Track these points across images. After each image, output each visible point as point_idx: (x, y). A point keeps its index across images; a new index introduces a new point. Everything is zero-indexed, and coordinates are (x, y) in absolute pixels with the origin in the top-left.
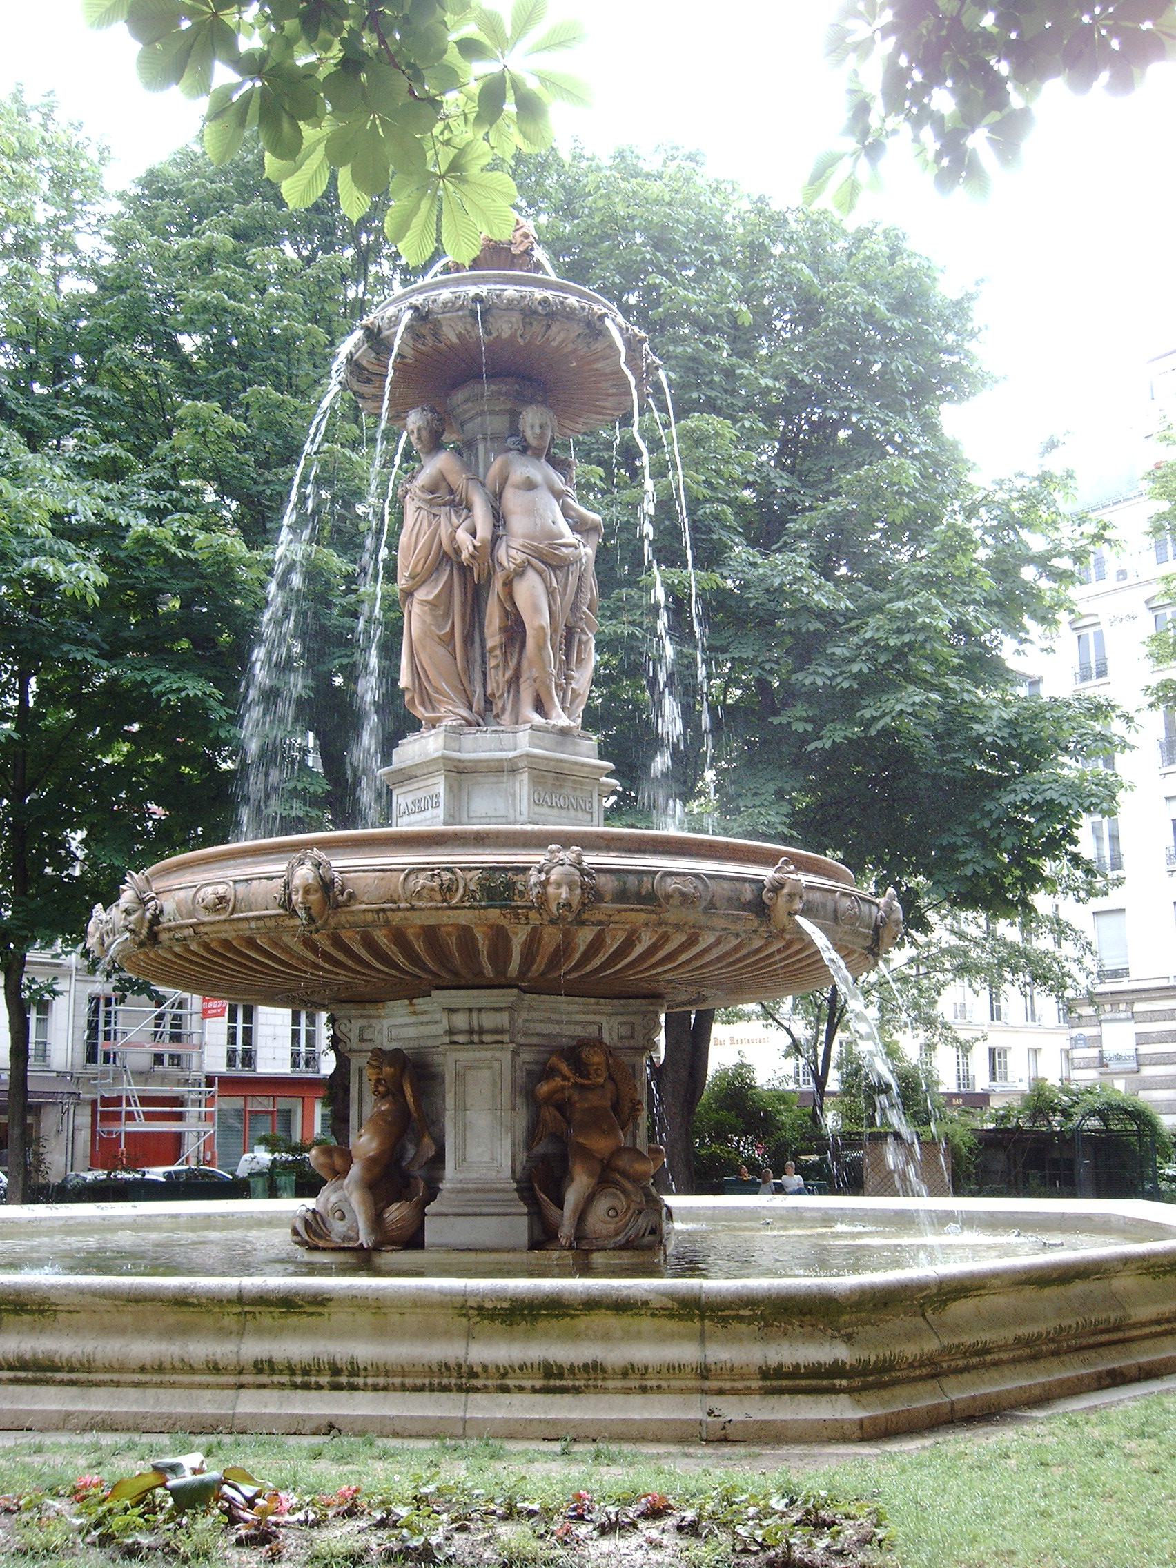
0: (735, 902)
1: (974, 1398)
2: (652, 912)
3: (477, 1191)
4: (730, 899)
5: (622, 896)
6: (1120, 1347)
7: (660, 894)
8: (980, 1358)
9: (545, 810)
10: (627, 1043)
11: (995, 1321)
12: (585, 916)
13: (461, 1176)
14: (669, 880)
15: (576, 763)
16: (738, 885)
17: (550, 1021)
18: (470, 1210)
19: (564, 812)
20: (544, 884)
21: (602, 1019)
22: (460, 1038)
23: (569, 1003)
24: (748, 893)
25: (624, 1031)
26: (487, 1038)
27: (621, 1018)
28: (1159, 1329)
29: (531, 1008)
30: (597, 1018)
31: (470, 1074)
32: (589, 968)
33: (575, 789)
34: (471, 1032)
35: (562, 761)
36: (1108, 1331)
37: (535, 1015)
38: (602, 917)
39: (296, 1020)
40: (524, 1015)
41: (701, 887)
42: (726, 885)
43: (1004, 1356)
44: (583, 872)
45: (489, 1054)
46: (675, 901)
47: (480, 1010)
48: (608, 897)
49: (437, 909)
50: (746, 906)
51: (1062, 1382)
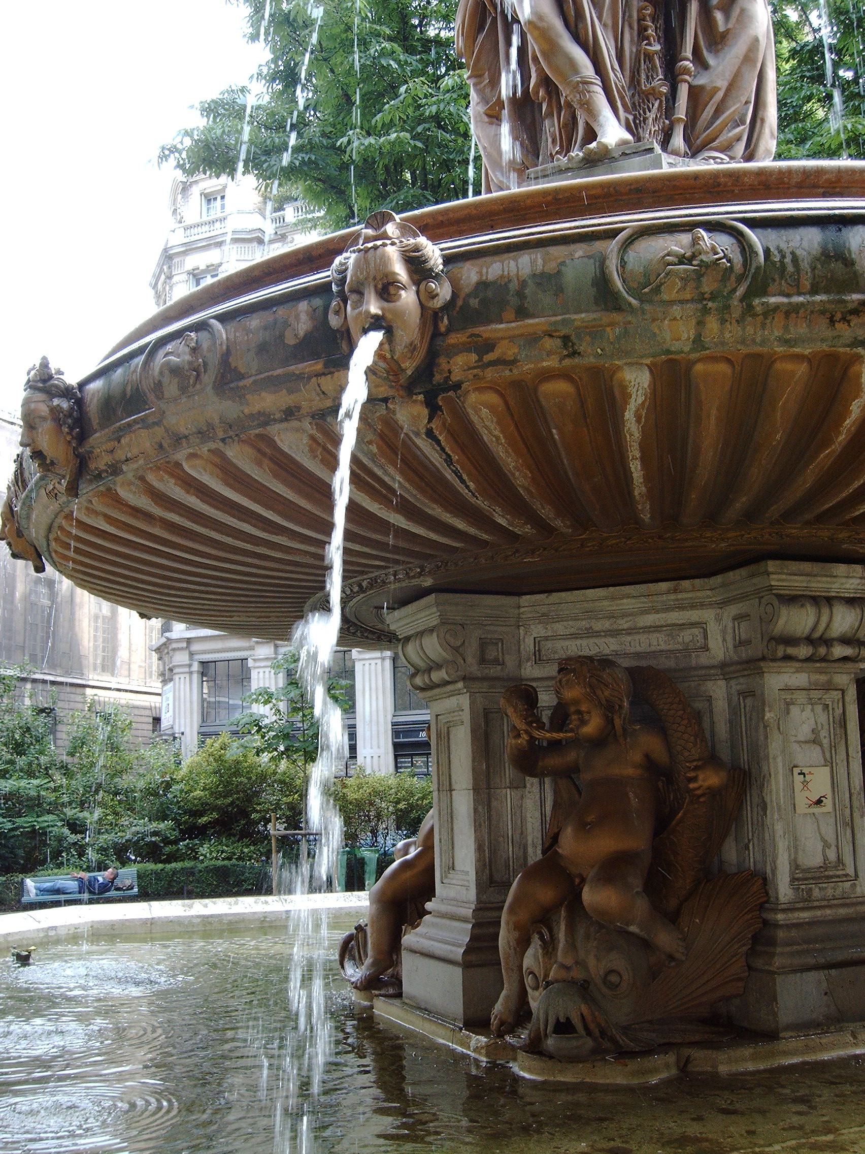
4: (262, 348)
10: (745, 653)
16: (281, 311)
17: (590, 633)
21: (708, 615)
23: (613, 598)
24: (301, 319)
25: (744, 630)
27: (734, 610)
29: (545, 618)
30: (694, 615)
31: (453, 731)
37: (560, 628)
40: (538, 630)
45: (451, 703)
46: (171, 389)
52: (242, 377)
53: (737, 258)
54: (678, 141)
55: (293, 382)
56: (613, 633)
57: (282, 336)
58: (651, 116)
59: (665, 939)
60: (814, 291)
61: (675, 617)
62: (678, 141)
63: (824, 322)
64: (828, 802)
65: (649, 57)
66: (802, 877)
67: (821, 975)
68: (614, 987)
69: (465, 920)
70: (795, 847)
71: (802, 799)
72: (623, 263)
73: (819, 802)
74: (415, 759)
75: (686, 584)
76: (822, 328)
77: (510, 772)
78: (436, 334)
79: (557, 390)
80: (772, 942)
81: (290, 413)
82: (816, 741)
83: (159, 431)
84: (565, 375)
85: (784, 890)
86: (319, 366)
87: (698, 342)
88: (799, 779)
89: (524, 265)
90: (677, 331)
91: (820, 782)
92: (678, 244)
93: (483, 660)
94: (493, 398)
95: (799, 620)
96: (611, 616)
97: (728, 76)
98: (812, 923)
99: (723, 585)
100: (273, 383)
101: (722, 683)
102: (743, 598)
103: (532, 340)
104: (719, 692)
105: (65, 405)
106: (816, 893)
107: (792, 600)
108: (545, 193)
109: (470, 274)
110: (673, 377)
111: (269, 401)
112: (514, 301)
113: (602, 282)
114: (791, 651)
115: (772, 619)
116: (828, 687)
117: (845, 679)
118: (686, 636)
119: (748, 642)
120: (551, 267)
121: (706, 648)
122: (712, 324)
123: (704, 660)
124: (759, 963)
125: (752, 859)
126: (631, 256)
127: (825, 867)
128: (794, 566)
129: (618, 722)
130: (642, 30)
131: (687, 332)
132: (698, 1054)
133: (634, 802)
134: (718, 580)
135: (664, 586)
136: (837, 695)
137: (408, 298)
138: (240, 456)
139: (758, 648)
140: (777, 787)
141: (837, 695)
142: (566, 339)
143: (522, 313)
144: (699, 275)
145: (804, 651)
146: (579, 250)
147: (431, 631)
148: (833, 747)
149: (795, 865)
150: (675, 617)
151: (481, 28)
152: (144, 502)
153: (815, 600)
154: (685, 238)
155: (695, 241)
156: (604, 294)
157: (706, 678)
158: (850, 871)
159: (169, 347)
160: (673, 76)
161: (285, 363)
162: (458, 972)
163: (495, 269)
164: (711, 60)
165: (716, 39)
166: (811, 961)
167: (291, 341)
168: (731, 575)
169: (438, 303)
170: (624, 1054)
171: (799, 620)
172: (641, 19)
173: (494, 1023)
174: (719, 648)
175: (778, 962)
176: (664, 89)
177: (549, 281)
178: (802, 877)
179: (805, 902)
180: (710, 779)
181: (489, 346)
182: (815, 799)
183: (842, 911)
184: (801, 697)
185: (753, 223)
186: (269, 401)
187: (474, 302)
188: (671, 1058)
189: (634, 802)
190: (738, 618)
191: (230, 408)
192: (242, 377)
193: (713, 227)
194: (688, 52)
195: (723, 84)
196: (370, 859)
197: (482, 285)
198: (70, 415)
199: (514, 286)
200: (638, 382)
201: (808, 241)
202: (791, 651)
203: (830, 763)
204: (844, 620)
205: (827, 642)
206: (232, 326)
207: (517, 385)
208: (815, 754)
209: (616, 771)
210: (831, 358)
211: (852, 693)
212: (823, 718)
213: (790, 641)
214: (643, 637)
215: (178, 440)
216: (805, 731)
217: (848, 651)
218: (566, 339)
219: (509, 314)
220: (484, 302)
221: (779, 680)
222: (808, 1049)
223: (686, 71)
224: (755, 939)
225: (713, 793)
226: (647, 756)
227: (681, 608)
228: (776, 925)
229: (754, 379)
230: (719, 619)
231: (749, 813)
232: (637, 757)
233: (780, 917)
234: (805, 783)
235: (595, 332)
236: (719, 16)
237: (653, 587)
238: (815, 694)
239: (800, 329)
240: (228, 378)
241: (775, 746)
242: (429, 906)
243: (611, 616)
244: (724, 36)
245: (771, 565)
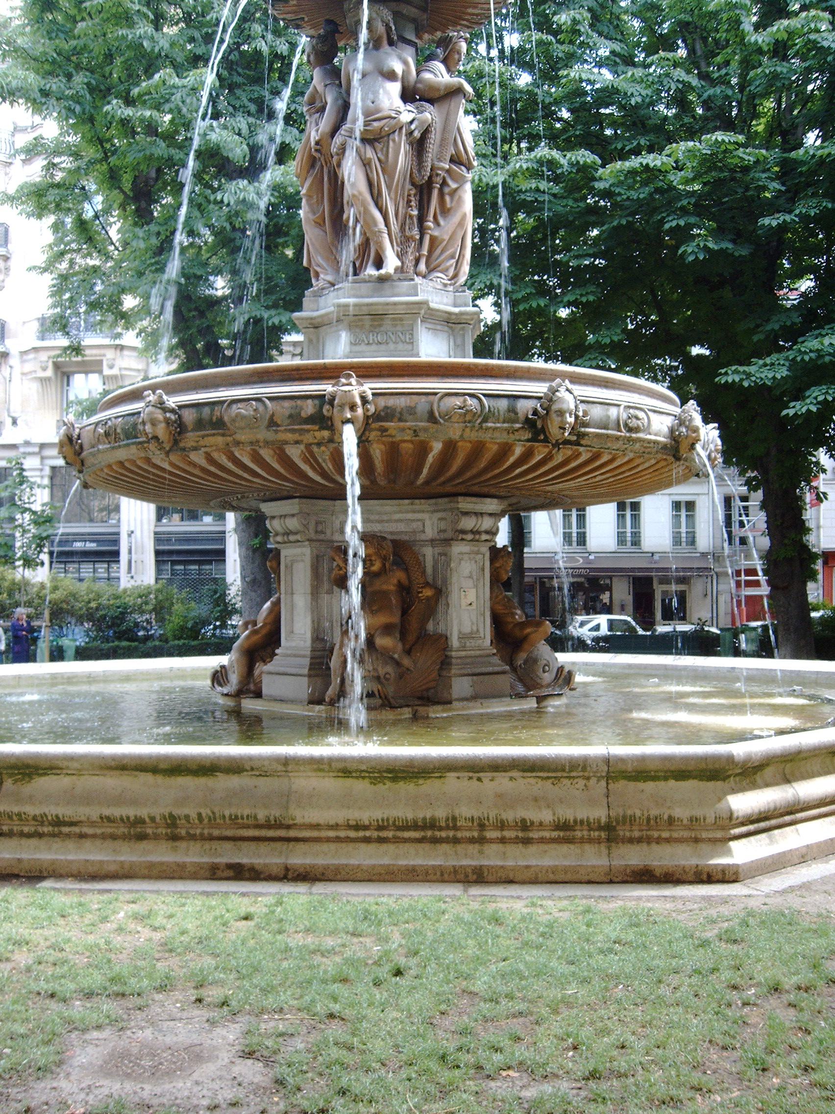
0: (295, 418)
1: (19, 860)
2: (223, 435)
3: (295, 656)
5: (200, 424)
6: (278, 845)
7: (226, 419)
8: (57, 828)
9: (363, 348)
10: (442, 536)
11: (88, 799)
12: (182, 445)
13: (288, 644)
14: (234, 406)
15: (387, 304)
16: (299, 402)
18: (282, 670)
19: (383, 347)
20: (144, 423)
21: (425, 516)
22: (279, 539)
24: (309, 408)
25: (443, 525)
26: (292, 538)
28: (352, 834)
32: (468, 475)
33: (395, 326)
34: (284, 534)
35: (371, 304)
36: (258, 826)
38: (194, 444)
39: (621, 517)
41: (261, 408)
42: (287, 404)
43: (89, 831)
44: (165, 410)
45: (298, 551)
47: (285, 516)
48: (190, 427)
49: (113, 448)
50: (311, 420)
51: (151, 865)
52: (278, 426)
53: (479, 408)
54: (422, 267)
55: (302, 432)
56: (381, 521)
57: (300, 414)
58: (410, 250)
59: (406, 662)
60: (504, 422)
61: (410, 516)
62: (422, 267)
63: (505, 433)
64: (474, 604)
65: (411, 217)
66: (462, 637)
67: (470, 678)
68: (387, 680)
69: (304, 656)
70: (460, 624)
71: (464, 603)
72: (439, 406)
74: (68, 565)
75: (417, 501)
76: (505, 434)
77: (326, 586)
78: (367, 424)
79: (407, 447)
80: (450, 664)
81: (297, 442)
82: (470, 577)
83: (229, 439)
84: (411, 442)
85: (455, 642)
86: (317, 428)
87: (462, 436)
89: (402, 402)
90: (455, 431)
91: (471, 596)
92: (458, 401)
93: (316, 532)
94: (382, 447)
95: (468, 523)
96: (379, 513)
97: (450, 233)
98: (466, 657)
99: (436, 504)
100: (293, 431)
101: (430, 548)
102: (445, 510)
103: (403, 430)
104: (428, 553)
105: (173, 417)
106: (468, 644)
107: (466, 514)
108: (404, 363)
109: (382, 402)
110: (450, 447)
111: (289, 436)
112: (398, 415)
113: (431, 413)
114: (464, 537)
115: (458, 522)
116: (478, 553)
117: (485, 549)
118: (414, 525)
119: (445, 531)
120: (413, 405)
121: (423, 532)
122: (468, 430)
123: (423, 537)
124: (444, 673)
125: (441, 628)
126: (442, 404)
127: (471, 633)
128: (469, 499)
129: (387, 566)
130: (409, 201)
131: (458, 433)
132: (420, 709)
133: (394, 602)
134: (433, 501)
135: (407, 501)
136: (481, 556)
137: (360, 411)
138: (266, 454)
139: (449, 535)
140: (454, 598)
141: (481, 556)
142: (415, 431)
143: (400, 420)
144: (465, 414)
145: (470, 537)
146: (423, 399)
147: (293, 515)
148: (478, 580)
149: (460, 632)
150: (410, 516)
151: (313, 166)
152: (203, 462)
153: (476, 514)
154: (461, 399)
155: (465, 401)
156: (431, 417)
157: (422, 546)
159: (239, 405)
160: (422, 230)
161: (300, 424)
162: (306, 679)
163: (391, 402)
164: (442, 222)
165: (445, 211)
166: (466, 672)
167: (303, 415)
168: (440, 500)
169: (370, 413)
170: (392, 707)
171: (468, 523)
172: (409, 195)
173: (327, 699)
174: (430, 532)
175: (453, 672)
176: (418, 237)
177: (411, 411)
178: (462, 637)
179: (463, 648)
180: (428, 592)
181: (386, 430)
183: (478, 653)
184: (466, 557)
186: (289, 436)
187: (382, 414)
188: (410, 709)
189: (394, 602)
190: (441, 519)
191: (270, 435)
192: (278, 426)
193: (472, 396)
194: (431, 218)
195: (446, 237)
196: (69, 647)
197: (386, 408)
198: (175, 422)
199: (399, 410)
200: (437, 447)
201: (503, 404)
202: (464, 537)
203: (476, 587)
205: (479, 533)
206: (275, 403)
207: (393, 443)
208: (470, 583)
209: (385, 587)
210: (507, 444)
211: (488, 555)
212: (474, 566)
213: (463, 532)
214: (394, 525)
215: (238, 443)
216: (466, 573)
218: (415, 431)
219: (396, 419)
220: (387, 413)
221: (458, 549)
222: (463, 708)
223: (430, 228)
224: (442, 663)
225: (428, 599)
226: (399, 581)
227: (414, 512)
228: (451, 657)
229: (478, 448)
230: (430, 519)
231: (441, 608)
232: (395, 581)
233: (453, 653)
235: (425, 430)
236: (447, 198)
237: (401, 501)
238: (472, 556)
239: (497, 434)
240: (272, 423)
241: (454, 579)
242: (277, 651)
243: (379, 513)
244: (449, 210)
245: (460, 499)
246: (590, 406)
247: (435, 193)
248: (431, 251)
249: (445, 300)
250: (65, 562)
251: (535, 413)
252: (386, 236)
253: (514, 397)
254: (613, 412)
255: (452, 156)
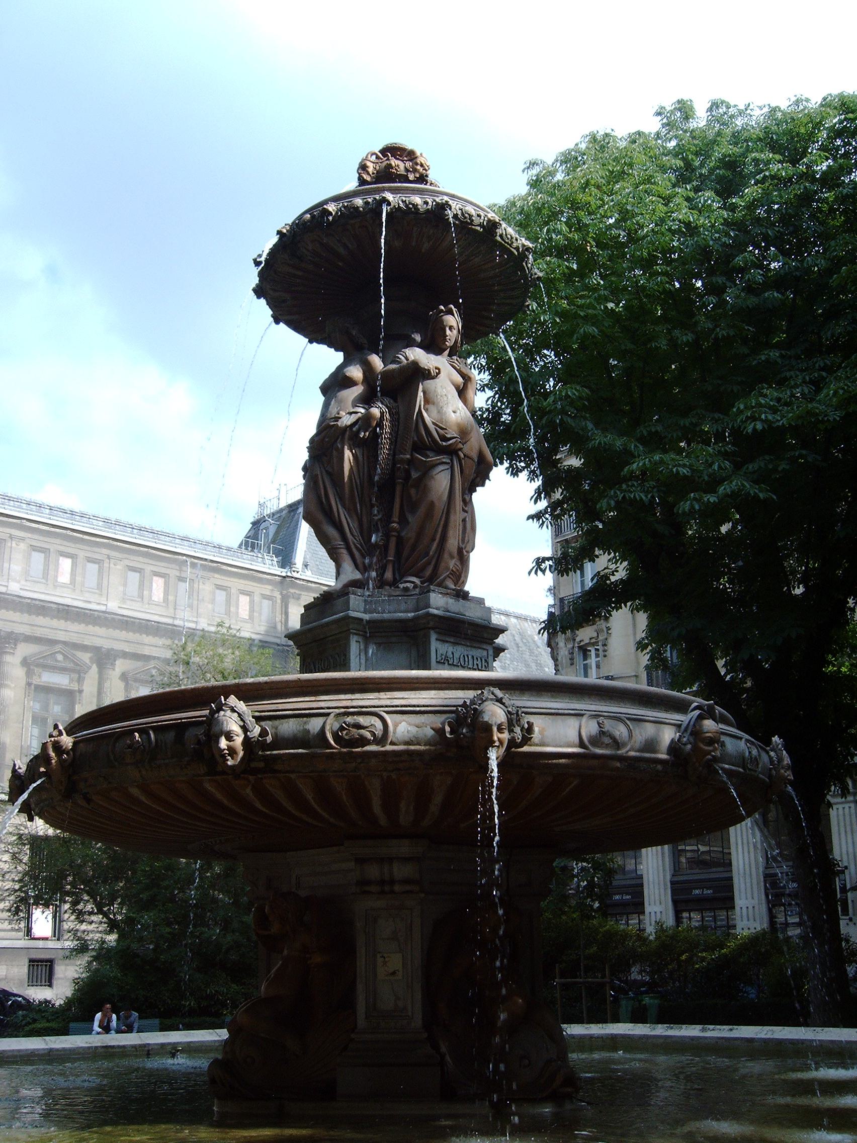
15: (322, 626)
54: (389, 575)
73: (394, 973)
88: (380, 960)
91: (395, 962)
95: (373, 872)
114: (367, 888)
135: (335, 849)
158: (410, 1014)
171: (373, 872)
182: (392, 971)
185: (155, 729)
202: (367, 888)
204: (400, 871)
205: (392, 882)
217: (408, 888)
223: (394, 530)
234: (385, 963)
236: (413, 491)
246: (277, 722)
247: (398, 489)
248: (398, 554)
249: (403, 607)
250: (714, 910)
251: (199, 742)
252: (344, 551)
253: (181, 727)
254: (315, 725)
255: (414, 443)
